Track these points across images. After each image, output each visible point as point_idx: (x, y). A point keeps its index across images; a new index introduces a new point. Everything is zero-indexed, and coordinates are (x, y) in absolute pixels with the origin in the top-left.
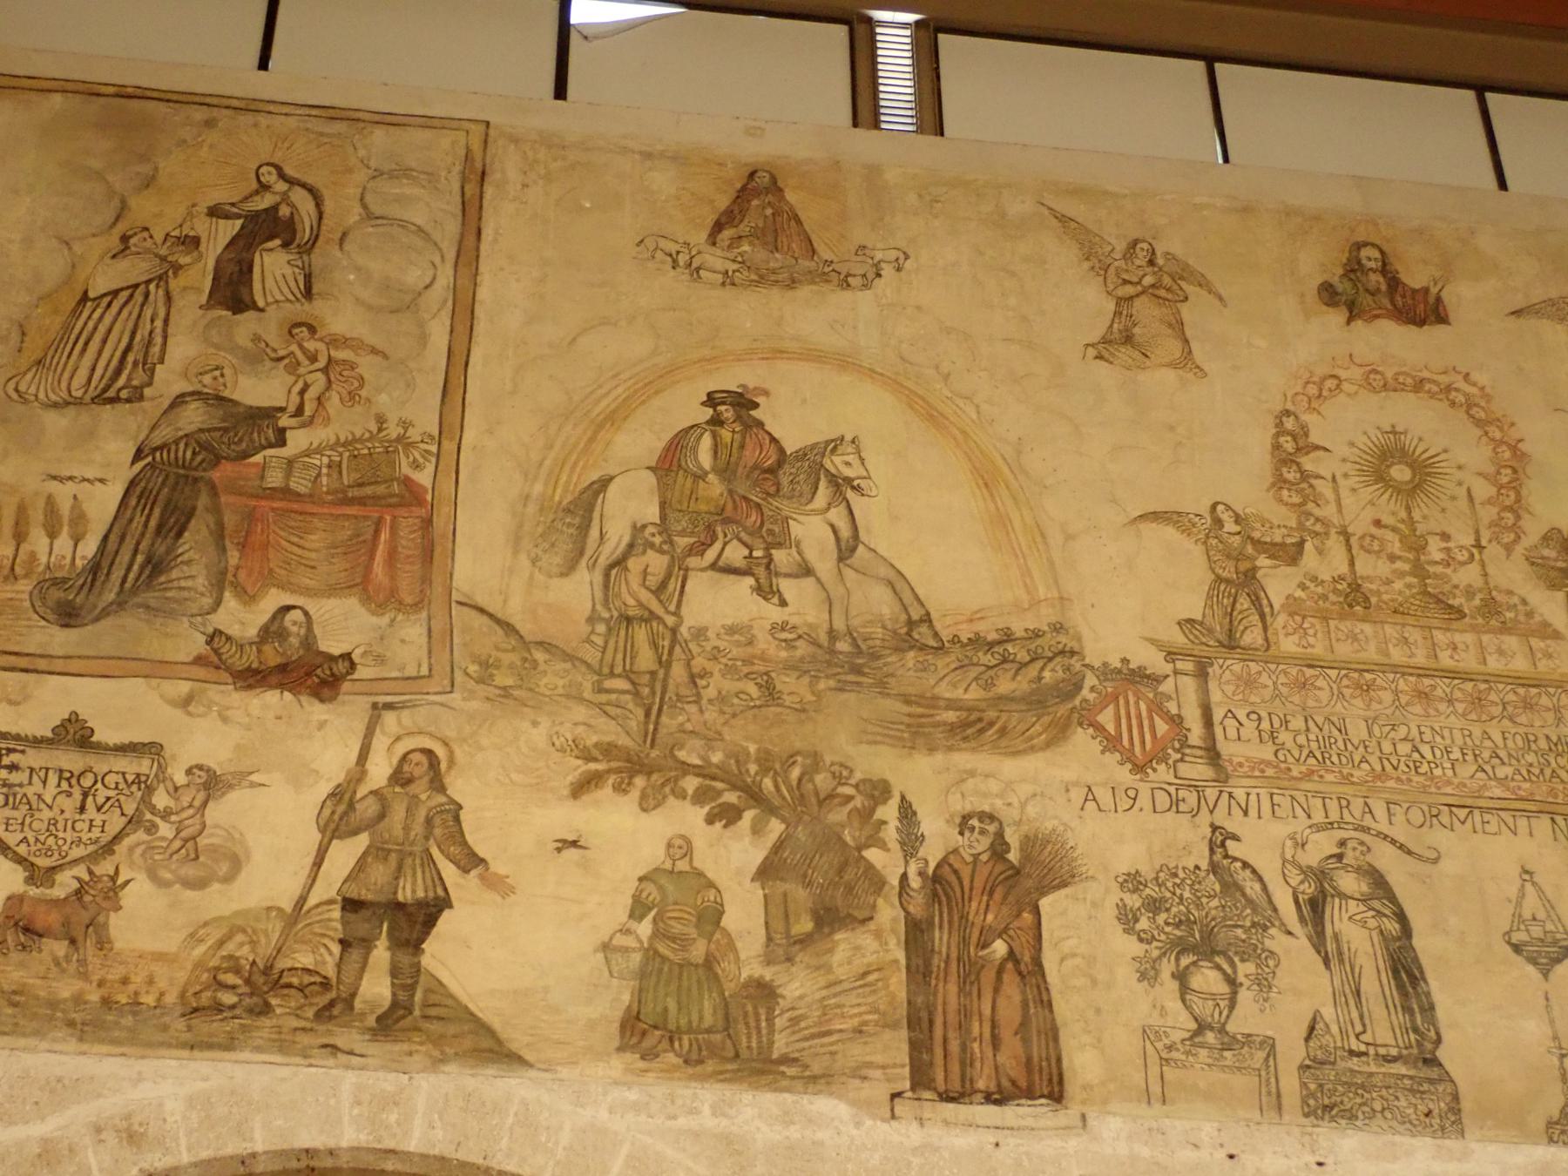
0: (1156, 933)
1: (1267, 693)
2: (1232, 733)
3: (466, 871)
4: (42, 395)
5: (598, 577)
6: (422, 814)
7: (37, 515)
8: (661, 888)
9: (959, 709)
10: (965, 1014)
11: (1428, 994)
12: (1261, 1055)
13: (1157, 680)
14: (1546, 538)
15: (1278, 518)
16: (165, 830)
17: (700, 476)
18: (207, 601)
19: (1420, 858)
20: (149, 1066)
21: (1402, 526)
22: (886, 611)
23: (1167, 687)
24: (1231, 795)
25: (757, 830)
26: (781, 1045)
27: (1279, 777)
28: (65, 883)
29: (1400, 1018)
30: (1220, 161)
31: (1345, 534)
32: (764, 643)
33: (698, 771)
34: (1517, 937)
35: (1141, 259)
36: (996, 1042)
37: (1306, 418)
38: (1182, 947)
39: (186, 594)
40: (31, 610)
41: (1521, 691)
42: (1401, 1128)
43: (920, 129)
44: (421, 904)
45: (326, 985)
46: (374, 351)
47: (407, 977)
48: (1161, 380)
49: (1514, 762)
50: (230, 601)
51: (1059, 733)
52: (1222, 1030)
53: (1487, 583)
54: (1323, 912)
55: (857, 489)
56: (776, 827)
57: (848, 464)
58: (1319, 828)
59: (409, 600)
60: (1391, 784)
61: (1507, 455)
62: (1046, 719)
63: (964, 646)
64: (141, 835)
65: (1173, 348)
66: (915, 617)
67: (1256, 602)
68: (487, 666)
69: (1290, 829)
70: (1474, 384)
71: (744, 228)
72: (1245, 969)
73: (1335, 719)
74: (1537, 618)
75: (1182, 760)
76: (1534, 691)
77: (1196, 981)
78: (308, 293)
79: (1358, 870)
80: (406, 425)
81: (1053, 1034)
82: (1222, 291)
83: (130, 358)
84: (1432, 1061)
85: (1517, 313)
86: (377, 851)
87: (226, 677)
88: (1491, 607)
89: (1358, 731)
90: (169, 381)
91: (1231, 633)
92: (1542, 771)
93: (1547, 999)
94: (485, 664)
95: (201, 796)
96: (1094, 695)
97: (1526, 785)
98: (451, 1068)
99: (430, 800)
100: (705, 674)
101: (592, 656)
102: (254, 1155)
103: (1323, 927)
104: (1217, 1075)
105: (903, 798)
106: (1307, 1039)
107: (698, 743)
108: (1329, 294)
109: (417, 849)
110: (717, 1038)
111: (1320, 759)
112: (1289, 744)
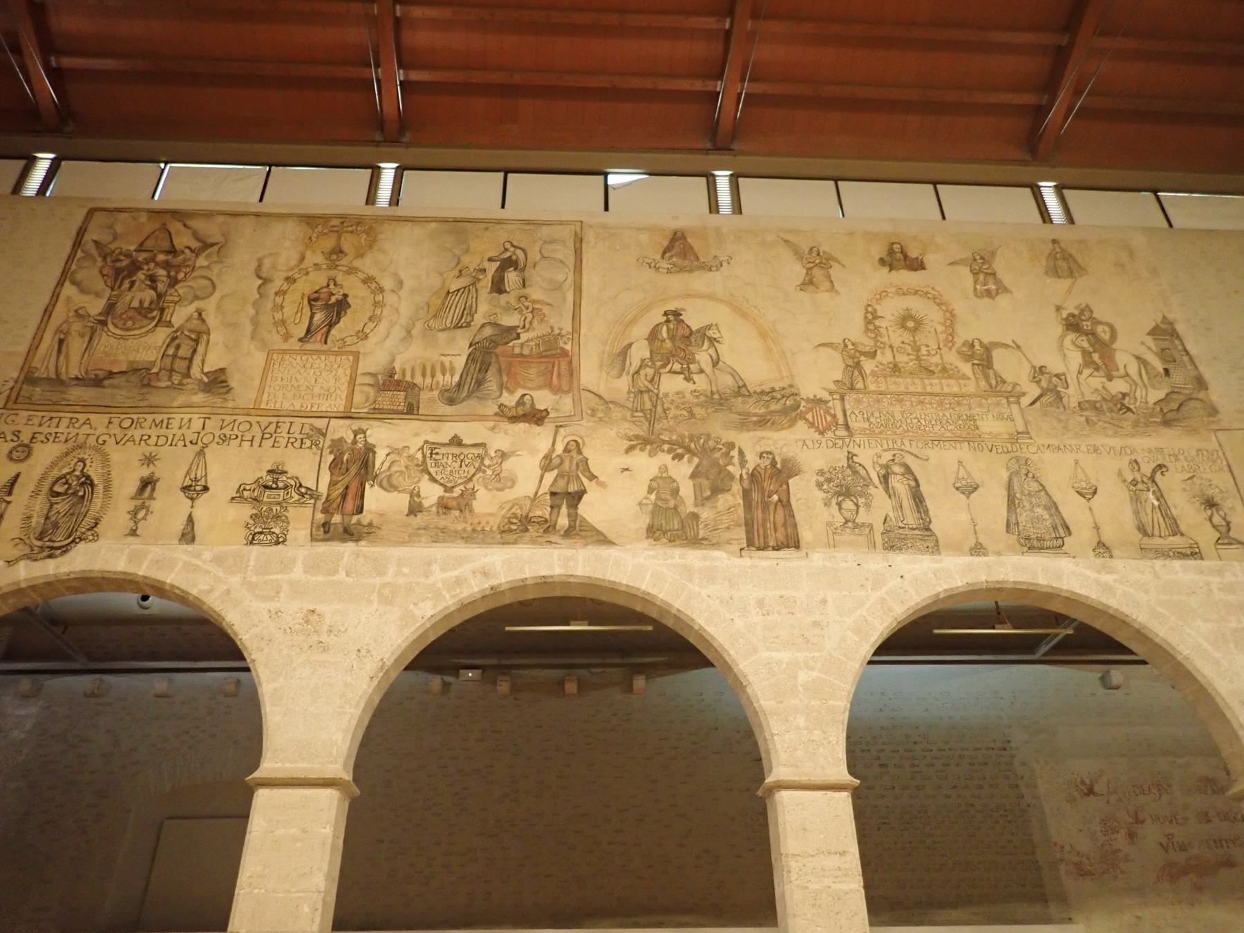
1: (866, 405)
2: (854, 419)
3: (591, 480)
5: (630, 377)
6: (575, 462)
7: (438, 368)
8: (658, 483)
10: (764, 520)
12: (868, 530)
13: (827, 402)
14: (964, 344)
15: (867, 343)
16: (489, 472)
17: (663, 341)
18: (498, 394)
19: (921, 459)
20: (490, 550)
23: (830, 404)
25: (690, 461)
26: (702, 534)
28: (457, 492)
29: (918, 515)
30: (841, 216)
31: (891, 347)
32: (689, 397)
33: (669, 443)
34: (957, 485)
35: (815, 254)
36: (776, 530)
38: (838, 494)
39: (490, 392)
43: (734, 213)
44: (576, 493)
45: (546, 521)
46: (548, 304)
47: (573, 517)
48: (823, 296)
50: (505, 394)
51: (793, 423)
52: (854, 522)
55: (718, 342)
56: (696, 460)
59: (566, 389)
60: (910, 434)
61: (949, 315)
62: (788, 418)
64: (481, 474)
65: (828, 284)
67: (861, 373)
68: (594, 412)
71: (673, 253)
72: (861, 501)
74: (961, 373)
77: (844, 506)
78: (524, 286)
80: (561, 329)
81: (795, 526)
83: (465, 312)
84: (928, 529)
86: (560, 475)
87: (506, 419)
88: (944, 370)
89: (898, 416)
90: (479, 319)
91: (852, 384)
94: (593, 410)
95: (500, 460)
98: (590, 547)
99: (578, 457)
100: (669, 409)
101: (630, 405)
102: (526, 579)
104: (853, 537)
105: (739, 448)
106: (884, 523)
107: (668, 433)
108: (882, 262)
109: (574, 474)
110: (680, 533)
112: (874, 422)
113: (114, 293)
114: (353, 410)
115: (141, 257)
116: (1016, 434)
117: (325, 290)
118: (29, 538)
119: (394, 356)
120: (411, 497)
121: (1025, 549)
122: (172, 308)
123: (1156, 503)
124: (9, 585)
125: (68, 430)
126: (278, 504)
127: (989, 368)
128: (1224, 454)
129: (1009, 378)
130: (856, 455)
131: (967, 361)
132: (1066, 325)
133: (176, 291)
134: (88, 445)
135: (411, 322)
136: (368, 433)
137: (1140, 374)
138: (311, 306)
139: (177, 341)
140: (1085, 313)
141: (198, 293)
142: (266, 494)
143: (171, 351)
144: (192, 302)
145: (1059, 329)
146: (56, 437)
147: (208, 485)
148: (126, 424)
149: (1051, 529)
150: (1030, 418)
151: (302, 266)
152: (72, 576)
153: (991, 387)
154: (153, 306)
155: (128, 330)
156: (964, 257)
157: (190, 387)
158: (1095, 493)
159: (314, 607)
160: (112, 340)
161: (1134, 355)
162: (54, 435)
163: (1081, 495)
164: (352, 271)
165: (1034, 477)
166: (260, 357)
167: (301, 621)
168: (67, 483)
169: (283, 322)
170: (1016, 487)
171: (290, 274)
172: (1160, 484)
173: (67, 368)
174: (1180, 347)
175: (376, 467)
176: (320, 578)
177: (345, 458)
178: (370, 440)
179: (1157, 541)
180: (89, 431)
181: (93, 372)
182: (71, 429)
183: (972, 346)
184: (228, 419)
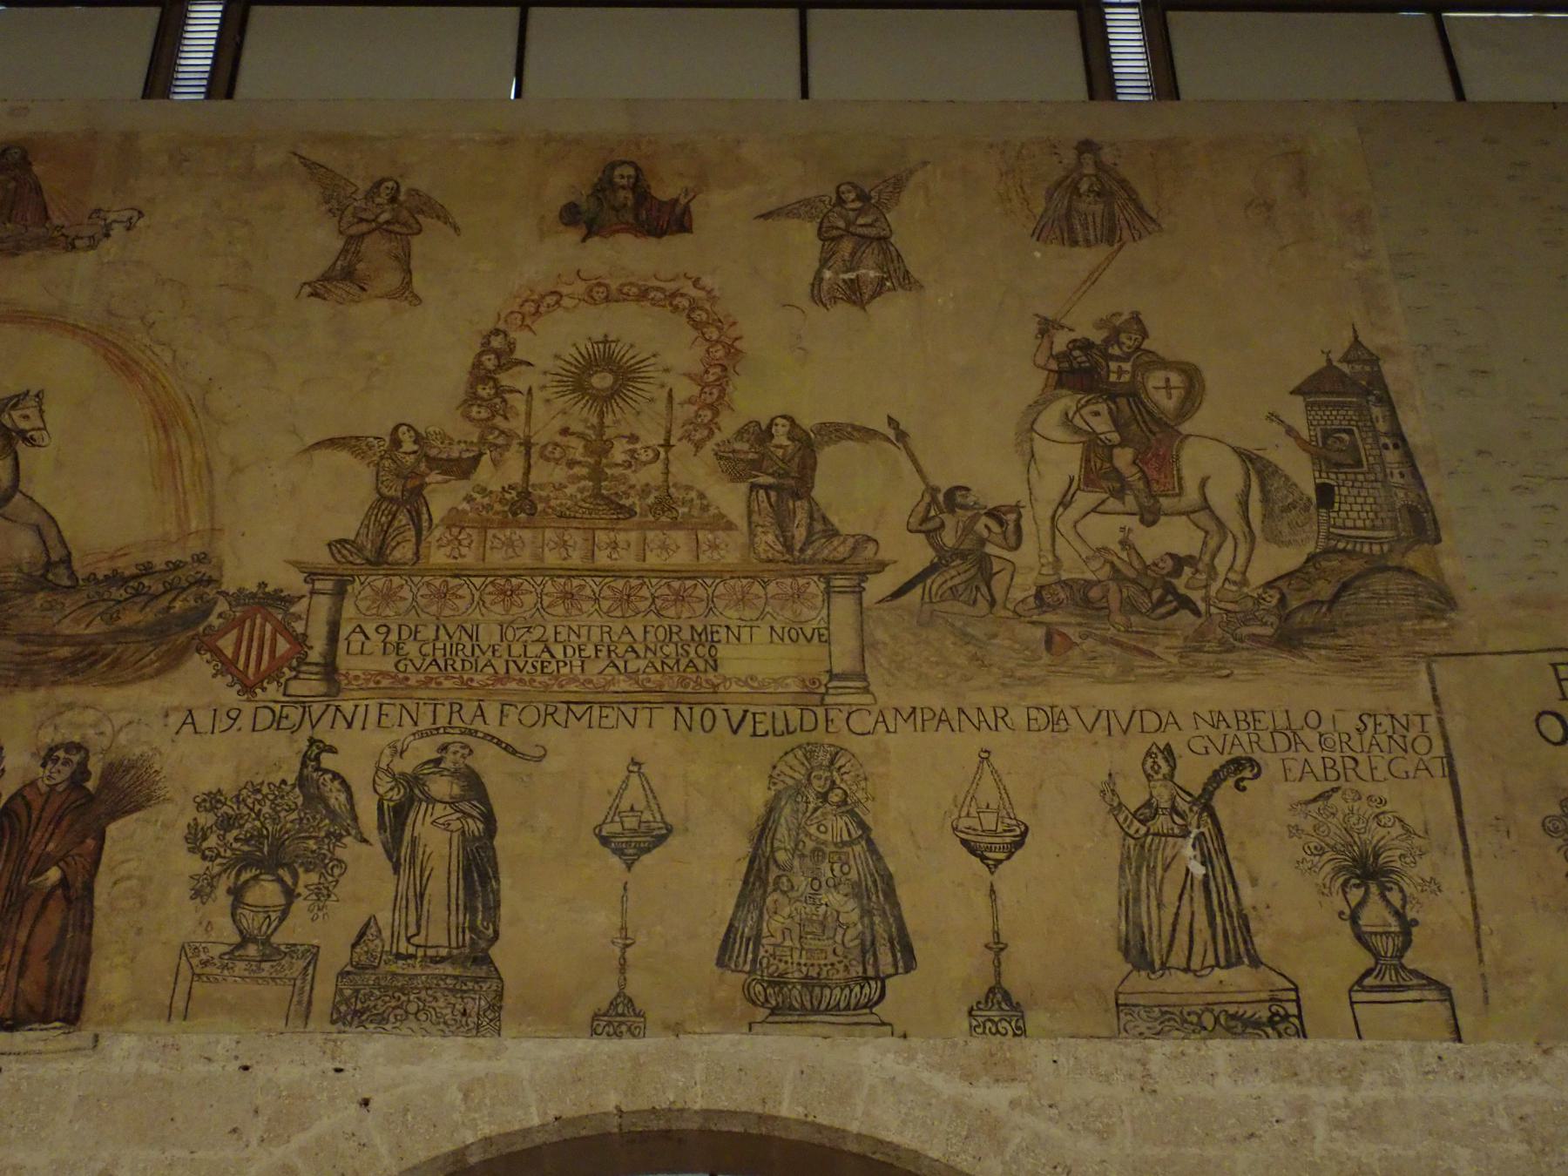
0: (222, 850)
1: (403, 606)
2: (356, 647)
9: (79, 644)
11: (496, 893)
12: (302, 964)
13: (291, 600)
14: (740, 433)
15: (461, 433)
19: (523, 756)
21: (588, 431)
22: (26, 554)
24: (338, 709)
27: (393, 687)
31: (527, 445)
35: (382, 199)
37: (513, 335)
38: (245, 862)
41: (676, 584)
42: (433, 1029)
49: (650, 655)
51: (174, 659)
52: (266, 942)
53: (666, 481)
54: (407, 816)
55: (25, 439)
57: (26, 417)
58: (422, 735)
60: (513, 685)
61: (721, 353)
63: (98, 582)
65: (393, 279)
66: (54, 557)
69: (394, 737)
70: (703, 289)
73: (468, 626)
74: (713, 511)
75: (296, 677)
76: (689, 583)
77: (251, 896)
79: (456, 774)
81: (84, 957)
82: (459, 221)
84: (485, 960)
85: (765, 216)
88: (665, 504)
89: (489, 635)
91: (380, 551)
92: (678, 662)
93: (625, 889)
96: (221, 620)
97: (658, 677)
103: (403, 830)
106: (354, 946)
108: (570, 215)
111: (442, 666)
116: (825, 678)
121: (762, 1013)
123: (1198, 870)
127: (796, 496)
128: (1441, 721)
129: (847, 522)
130: (332, 750)
131: (736, 478)
132: (1060, 372)
137: (1244, 505)
140: (1123, 338)
145: (1035, 382)
149: (856, 952)
150: (880, 635)
153: (789, 548)
156: (811, 193)
158: (1019, 843)
161: (1234, 449)
163: (973, 852)
165: (845, 802)
170: (782, 831)
172: (1222, 814)
174: (1382, 426)
179: (1177, 982)
183: (767, 434)
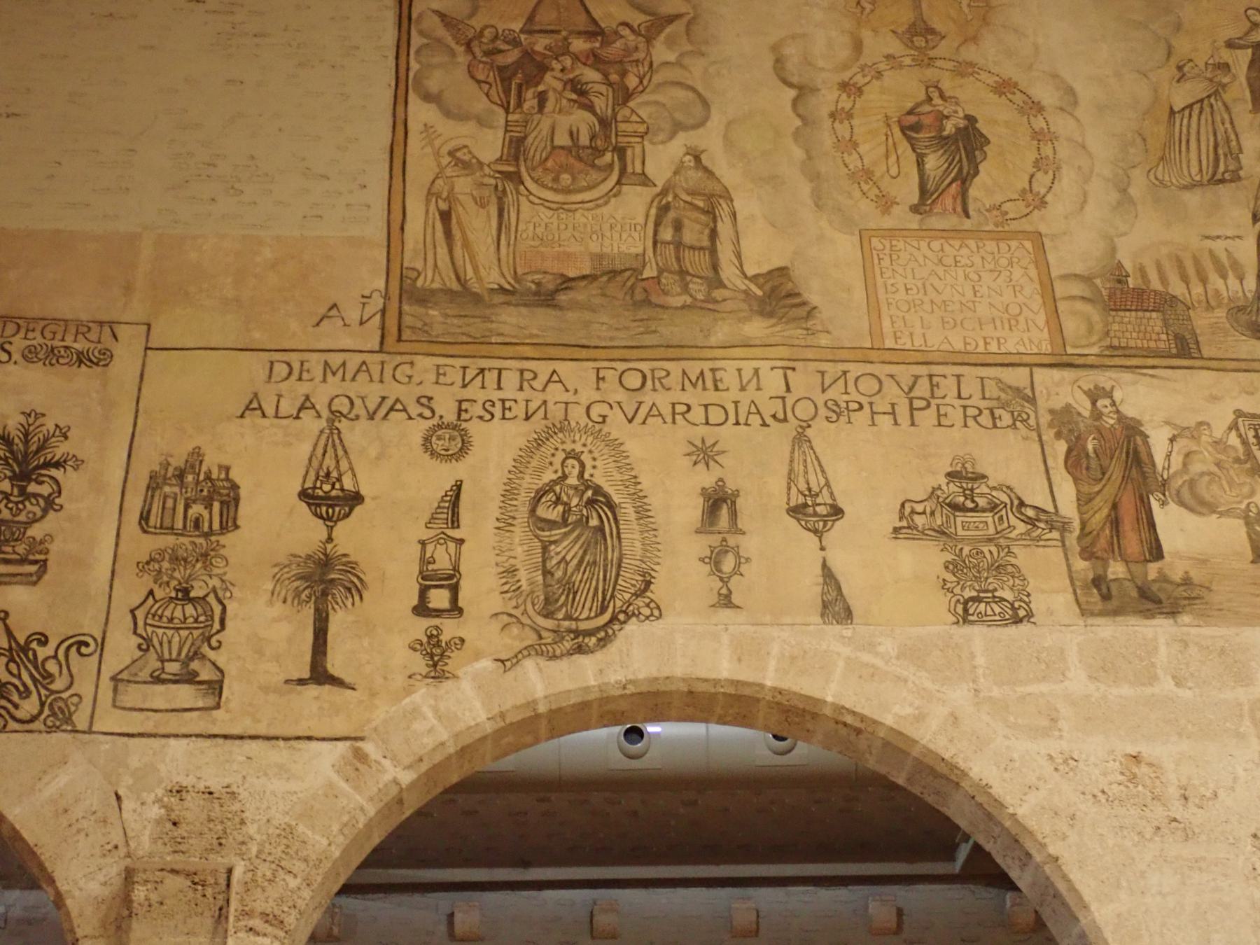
4: (1174, 181)
40: (1232, 330)
83: (1220, 152)
113: (511, 117)
114: (1070, 350)
115: (541, 44)
117: (927, 108)
118: (525, 612)
119: (1112, 241)
120: (1247, 524)
122: (638, 149)
124: (516, 707)
125: (521, 396)
126: (990, 540)
133: (633, 111)
134: (573, 424)
135: (1120, 171)
136: (1118, 395)
138: (909, 139)
139: (672, 215)
141: (679, 116)
142: (959, 520)
143: (667, 234)
144: (672, 136)
146: (504, 409)
147: (841, 505)
148: (633, 381)
151: (862, 61)
152: (631, 689)
154: (599, 143)
155: (567, 191)
157: (729, 305)
159: (1138, 749)
160: (545, 214)
162: (499, 405)
164: (965, 69)
166: (845, 246)
167: (1121, 778)
168: (558, 501)
169: (868, 174)
171: (846, 76)
173: (476, 269)
175: (1159, 468)
176: (1126, 690)
177: (1090, 447)
178: (1129, 411)
180: (568, 397)
181: (530, 278)
182: (527, 393)
184: (832, 370)
